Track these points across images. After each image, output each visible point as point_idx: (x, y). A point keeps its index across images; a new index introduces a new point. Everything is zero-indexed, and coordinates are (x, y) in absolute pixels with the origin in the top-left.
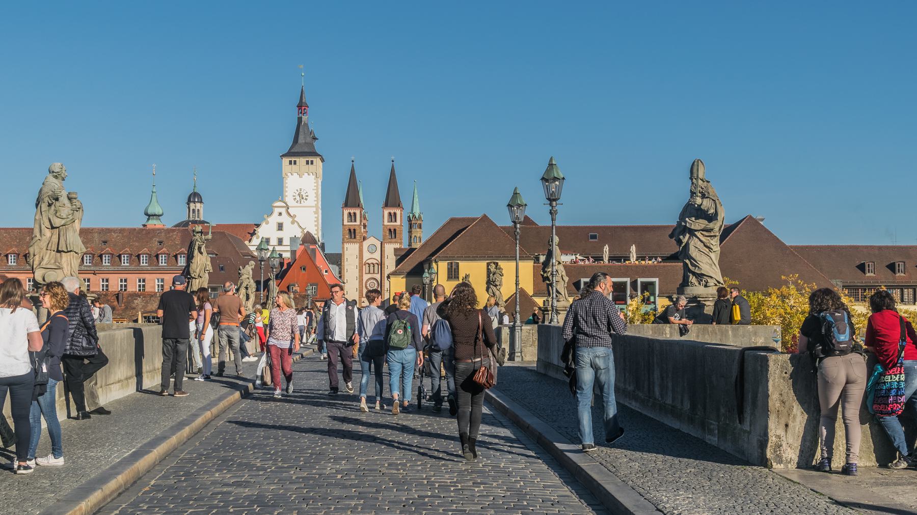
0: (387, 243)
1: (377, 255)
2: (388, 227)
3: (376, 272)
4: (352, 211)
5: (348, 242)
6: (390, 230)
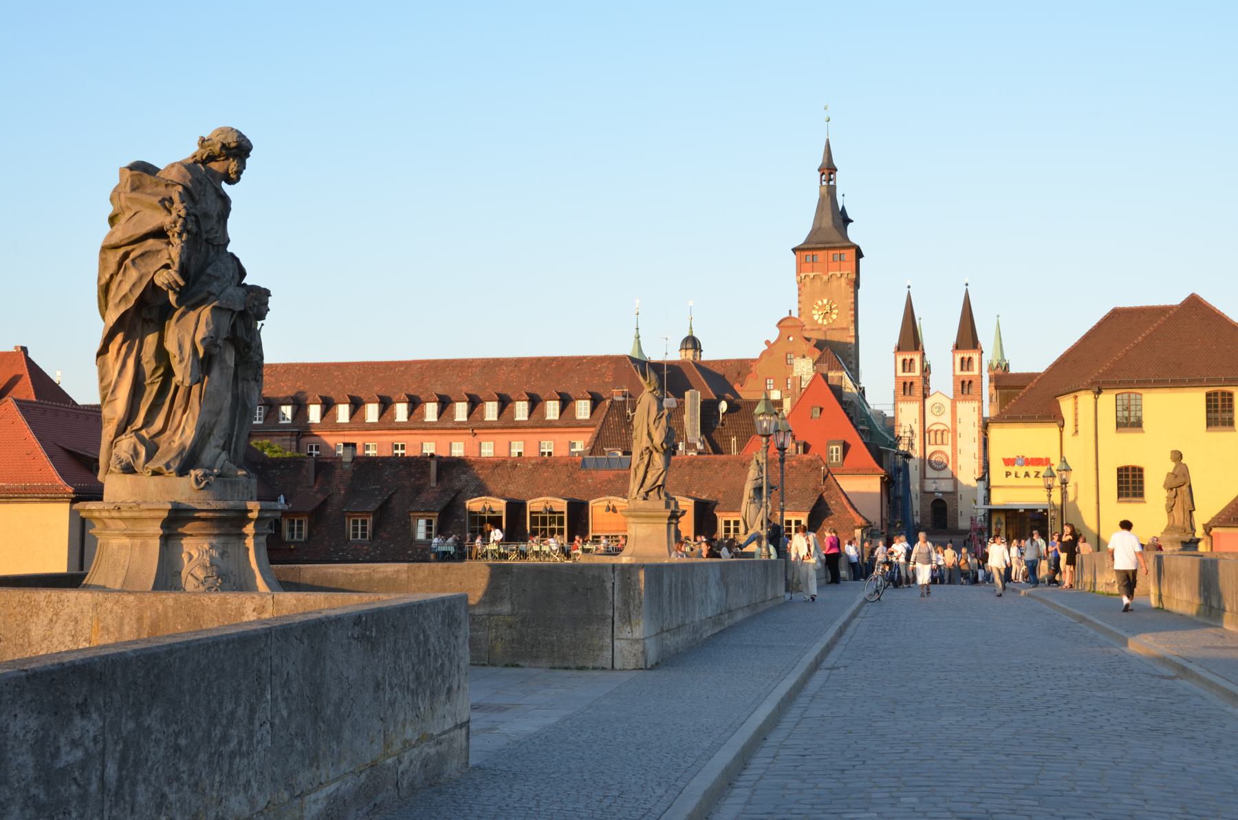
0: (959, 401)
1: (946, 419)
2: (961, 380)
3: (945, 442)
4: (908, 357)
5: (903, 401)
6: (963, 382)
